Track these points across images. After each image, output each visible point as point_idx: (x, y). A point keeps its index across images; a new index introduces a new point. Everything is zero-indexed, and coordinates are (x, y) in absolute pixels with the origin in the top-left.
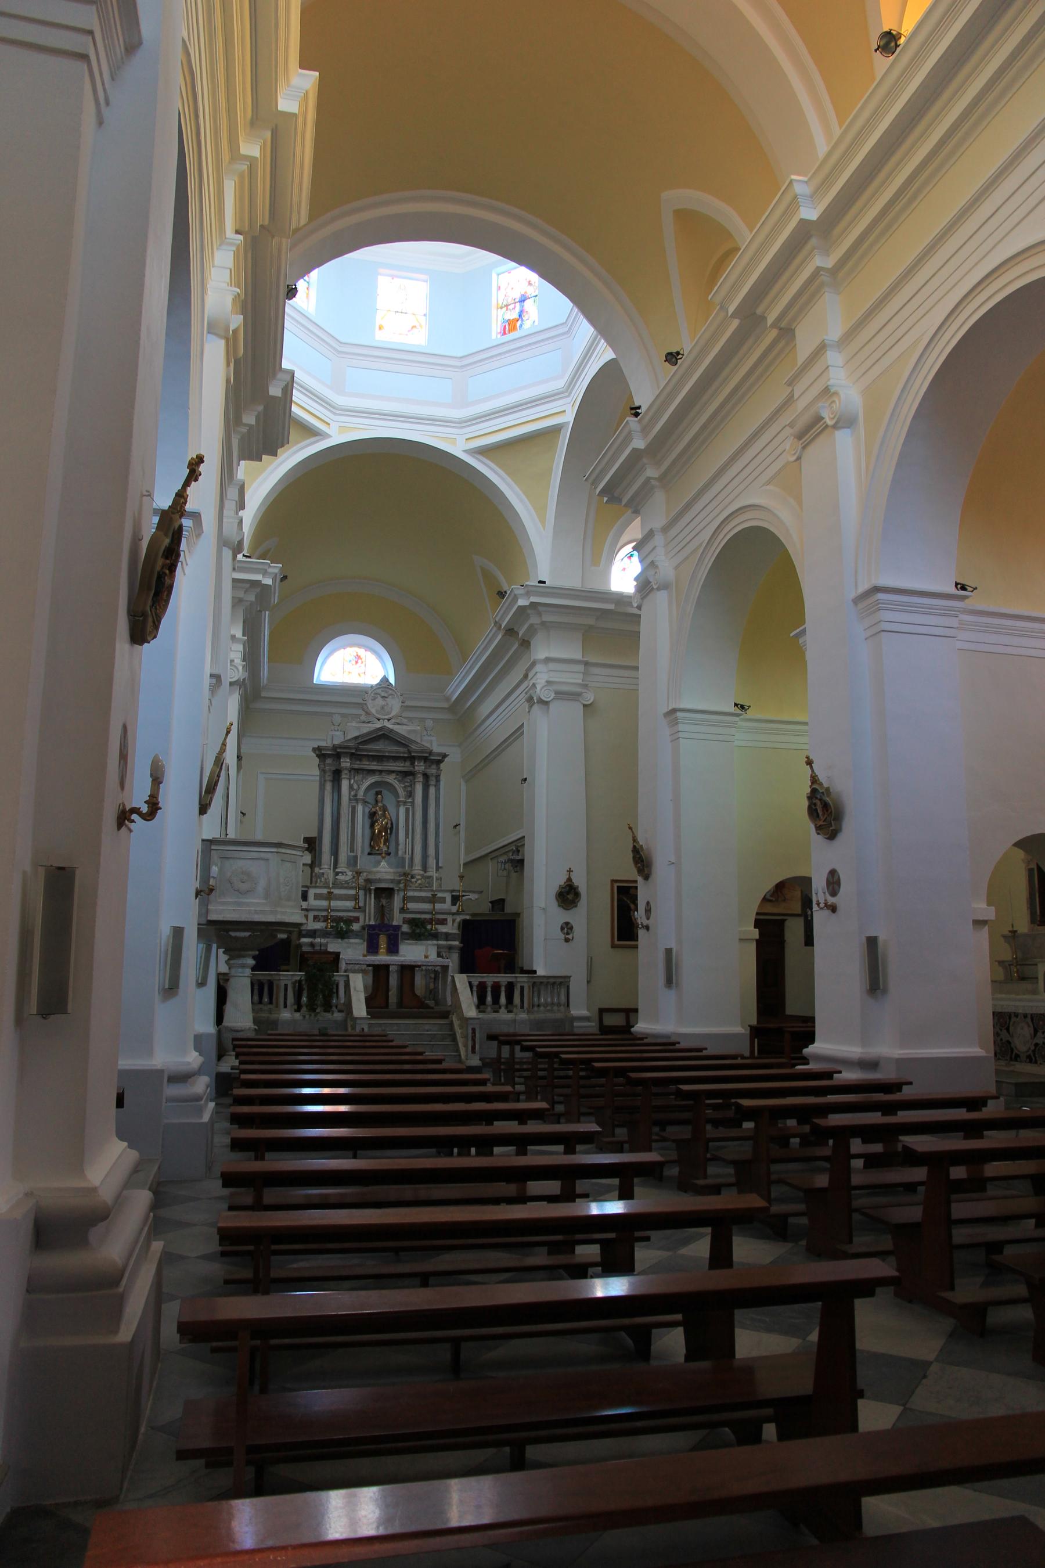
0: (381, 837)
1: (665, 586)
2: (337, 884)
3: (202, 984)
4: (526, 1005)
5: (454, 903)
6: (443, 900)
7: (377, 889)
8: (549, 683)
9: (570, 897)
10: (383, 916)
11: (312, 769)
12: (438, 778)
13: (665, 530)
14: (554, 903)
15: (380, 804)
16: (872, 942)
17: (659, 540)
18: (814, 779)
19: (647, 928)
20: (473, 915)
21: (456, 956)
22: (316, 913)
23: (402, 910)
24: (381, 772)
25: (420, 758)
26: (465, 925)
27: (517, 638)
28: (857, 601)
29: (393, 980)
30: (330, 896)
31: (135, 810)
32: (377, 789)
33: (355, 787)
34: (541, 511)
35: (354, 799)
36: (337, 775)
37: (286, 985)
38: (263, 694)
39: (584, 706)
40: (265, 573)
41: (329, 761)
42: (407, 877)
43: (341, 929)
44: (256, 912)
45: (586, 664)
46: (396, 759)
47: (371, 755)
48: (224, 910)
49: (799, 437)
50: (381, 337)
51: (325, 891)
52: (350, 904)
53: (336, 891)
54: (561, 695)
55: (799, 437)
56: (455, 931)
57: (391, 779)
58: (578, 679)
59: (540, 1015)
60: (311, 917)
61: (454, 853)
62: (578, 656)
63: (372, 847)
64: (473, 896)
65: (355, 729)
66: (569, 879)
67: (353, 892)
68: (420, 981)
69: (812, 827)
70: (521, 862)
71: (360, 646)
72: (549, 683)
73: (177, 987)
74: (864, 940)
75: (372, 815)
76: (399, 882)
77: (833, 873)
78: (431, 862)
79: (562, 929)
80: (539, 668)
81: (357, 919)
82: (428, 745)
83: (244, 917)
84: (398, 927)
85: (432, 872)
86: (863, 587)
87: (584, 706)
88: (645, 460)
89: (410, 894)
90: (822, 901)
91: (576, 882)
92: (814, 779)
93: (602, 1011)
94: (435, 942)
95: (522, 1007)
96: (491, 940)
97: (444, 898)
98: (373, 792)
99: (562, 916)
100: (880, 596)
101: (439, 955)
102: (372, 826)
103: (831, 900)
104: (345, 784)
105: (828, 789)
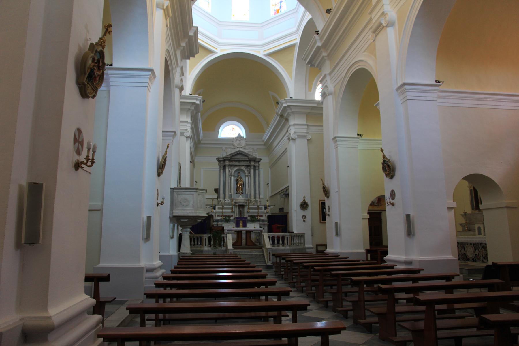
0: (240, 188)
1: (331, 94)
2: (225, 204)
3: (172, 238)
5: (265, 210)
6: (261, 209)
8: (295, 132)
9: (305, 206)
10: (241, 214)
11: (216, 166)
12: (259, 167)
13: (330, 74)
14: (299, 208)
16: (408, 216)
17: (328, 78)
18: (384, 157)
19: (329, 215)
20: (272, 213)
21: (266, 228)
23: (248, 212)
24: (239, 165)
25: (252, 160)
26: (269, 217)
27: (284, 118)
28: (398, 89)
29: (244, 236)
30: (223, 208)
31: (82, 163)
32: (239, 171)
34: (290, 73)
36: (224, 167)
38: (202, 142)
39: (308, 140)
40: (197, 100)
41: (222, 162)
42: (249, 201)
43: (227, 219)
44: (190, 213)
45: (308, 125)
47: (237, 161)
48: (179, 212)
49: (374, 32)
50: (233, 19)
51: (221, 206)
52: (230, 211)
53: (225, 206)
54: (299, 137)
55: (374, 32)
56: (266, 219)
57: (243, 168)
58: (305, 131)
59: (295, 247)
60: (217, 215)
61: (265, 193)
62: (305, 123)
63: (237, 191)
64: (272, 207)
65: (230, 151)
66: (304, 200)
67: (230, 206)
68: (253, 237)
69: (384, 174)
70: (288, 194)
71: (234, 125)
72: (295, 132)
73: (149, 238)
74: (405, 216)
75: (237, 180)
76: (246, 203)
77: (392, 191)
78: (257, 196)
80: (291, 127)
81: (232, 216)
82: (255, 156)
83: (185, 214)
84: (246, 218)
85: (258, 199)
86: (400, 84)
87: (308, 140)
88: (322, 50)
89: (250, 207)
90: (389, 202)
91: (307, 201)
92: (384, 157)
93: (317, 245)
96: (279, 222)
98: (237, 173)
99: (302, 213)
100: (406, 87)
101: (260, 227)
102: (237, 184)
103: (392, 201)
104: (227, 170)
105: (389, 160)
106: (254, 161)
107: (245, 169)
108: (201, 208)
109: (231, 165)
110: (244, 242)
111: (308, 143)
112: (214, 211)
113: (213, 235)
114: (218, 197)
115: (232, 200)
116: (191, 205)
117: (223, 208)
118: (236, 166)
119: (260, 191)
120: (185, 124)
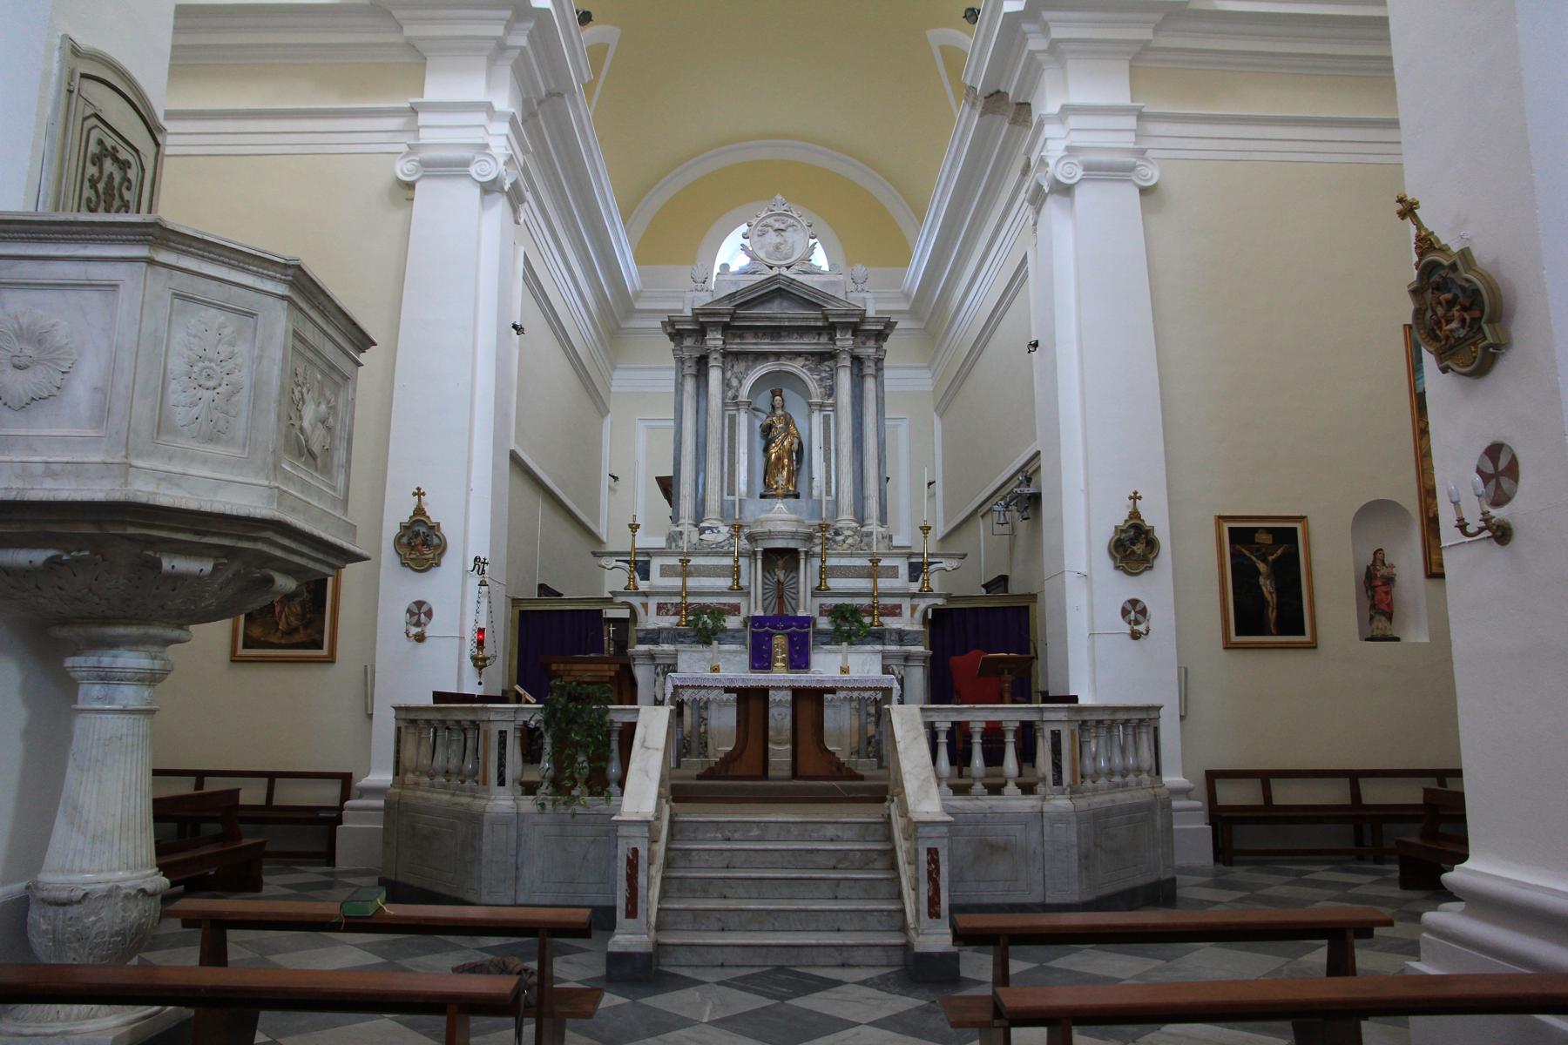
0: (784, 467)
4: (1066, 777)
6: (893, 572)
7: (768, 553)
9: (1139, 548)
10: (780, 598)
12: (879, 362)
14: (1104, 563)
15: (779, 412)
20: (949, 597)
21: (917, 677)
22: (663, 600)
23: (819, 591)
24: (778, 355)
25: (845, 326)
29: (780, 716)
30: (685, 571)
32: (775, 384)
33: (735, 382)
35: (732, 403)
36: (702, 362)
37: (503, 734)
38: (638, 306)
39: (1144, 191)
41: (688, 342)
42: (825, 532)
43: (702, 627)
44: (50, 470)
45: (1141, 116)
46: (803, 331)
52: (728, 582)
53: (694, 561)
54: (1098, 172)
56: (918, 627)
57: (796, 367)
58: (1128, 140)
59: (1102, 798)
60: (653, 608)
61: (914, 509)
62: (1124, 99)
63: (767, 485)
64: (948, 564)
66: (1135, 514)
67: (728, 561)
68: (839, 722)
70: (1035, 500)
75: (767, 430)
76: (809, 538)
79: (1125, 613)
81: (735, 609)
84: (807, 621)
85: (873, 526)
87: (1144, 191)
89: (831, 562)
91: (1148, 519)
93: (1212, 777)
94: (879, 647)
95: (1058, 781)
96: (985, 645)
97: (895, 568)
98: (768, 393)
101: (886, 670)
102: (766, 450)
104: (715, 376)
106: (856, 330)
107: (805, 374)
108: (214, 436)
109: (739, 355)
110: (780, 753)
111: (1145, 209)
112: (643, 586)
113: (550, 717)
114: (675, 519)
115: (737, 528)
116: (81, 391)
117: (685, 571)
119: (890, 485)
120: (481, 118)
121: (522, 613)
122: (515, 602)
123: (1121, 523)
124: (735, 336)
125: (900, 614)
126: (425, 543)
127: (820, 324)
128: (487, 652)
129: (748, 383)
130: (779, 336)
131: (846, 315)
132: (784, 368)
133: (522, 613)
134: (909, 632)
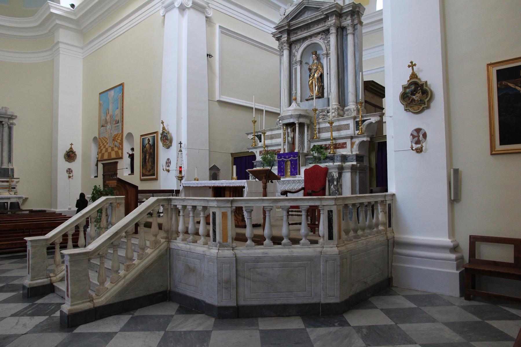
6: (347, 127)
24: (311, 36)
57: (317, 40)
60: (258, 153)
84: (297, 154)
91: (423, 77)
93: (474, 240)
97: (348, 125)
118: (305, 39)
121: (234, 158)
122: (232, 154)
123: (405, 83)
124: (294, 34)
125: (346, 147)
126: (167, 139)
127: (323, 17)
128: (183, 175)
129: (300, 51)
130: (310, 28)
131: (330, 9)
132: (312, 42)
133: (234, 158)
134: (349, 156)
